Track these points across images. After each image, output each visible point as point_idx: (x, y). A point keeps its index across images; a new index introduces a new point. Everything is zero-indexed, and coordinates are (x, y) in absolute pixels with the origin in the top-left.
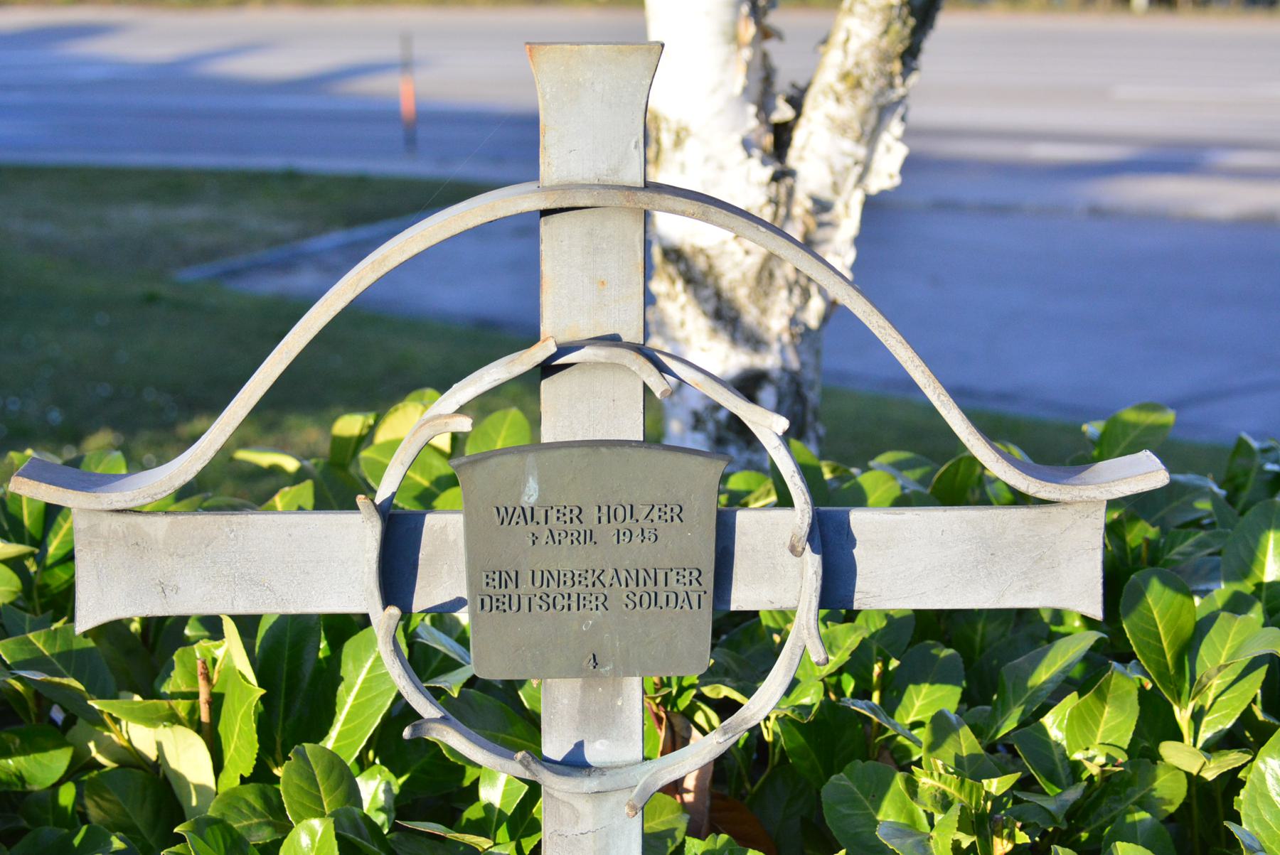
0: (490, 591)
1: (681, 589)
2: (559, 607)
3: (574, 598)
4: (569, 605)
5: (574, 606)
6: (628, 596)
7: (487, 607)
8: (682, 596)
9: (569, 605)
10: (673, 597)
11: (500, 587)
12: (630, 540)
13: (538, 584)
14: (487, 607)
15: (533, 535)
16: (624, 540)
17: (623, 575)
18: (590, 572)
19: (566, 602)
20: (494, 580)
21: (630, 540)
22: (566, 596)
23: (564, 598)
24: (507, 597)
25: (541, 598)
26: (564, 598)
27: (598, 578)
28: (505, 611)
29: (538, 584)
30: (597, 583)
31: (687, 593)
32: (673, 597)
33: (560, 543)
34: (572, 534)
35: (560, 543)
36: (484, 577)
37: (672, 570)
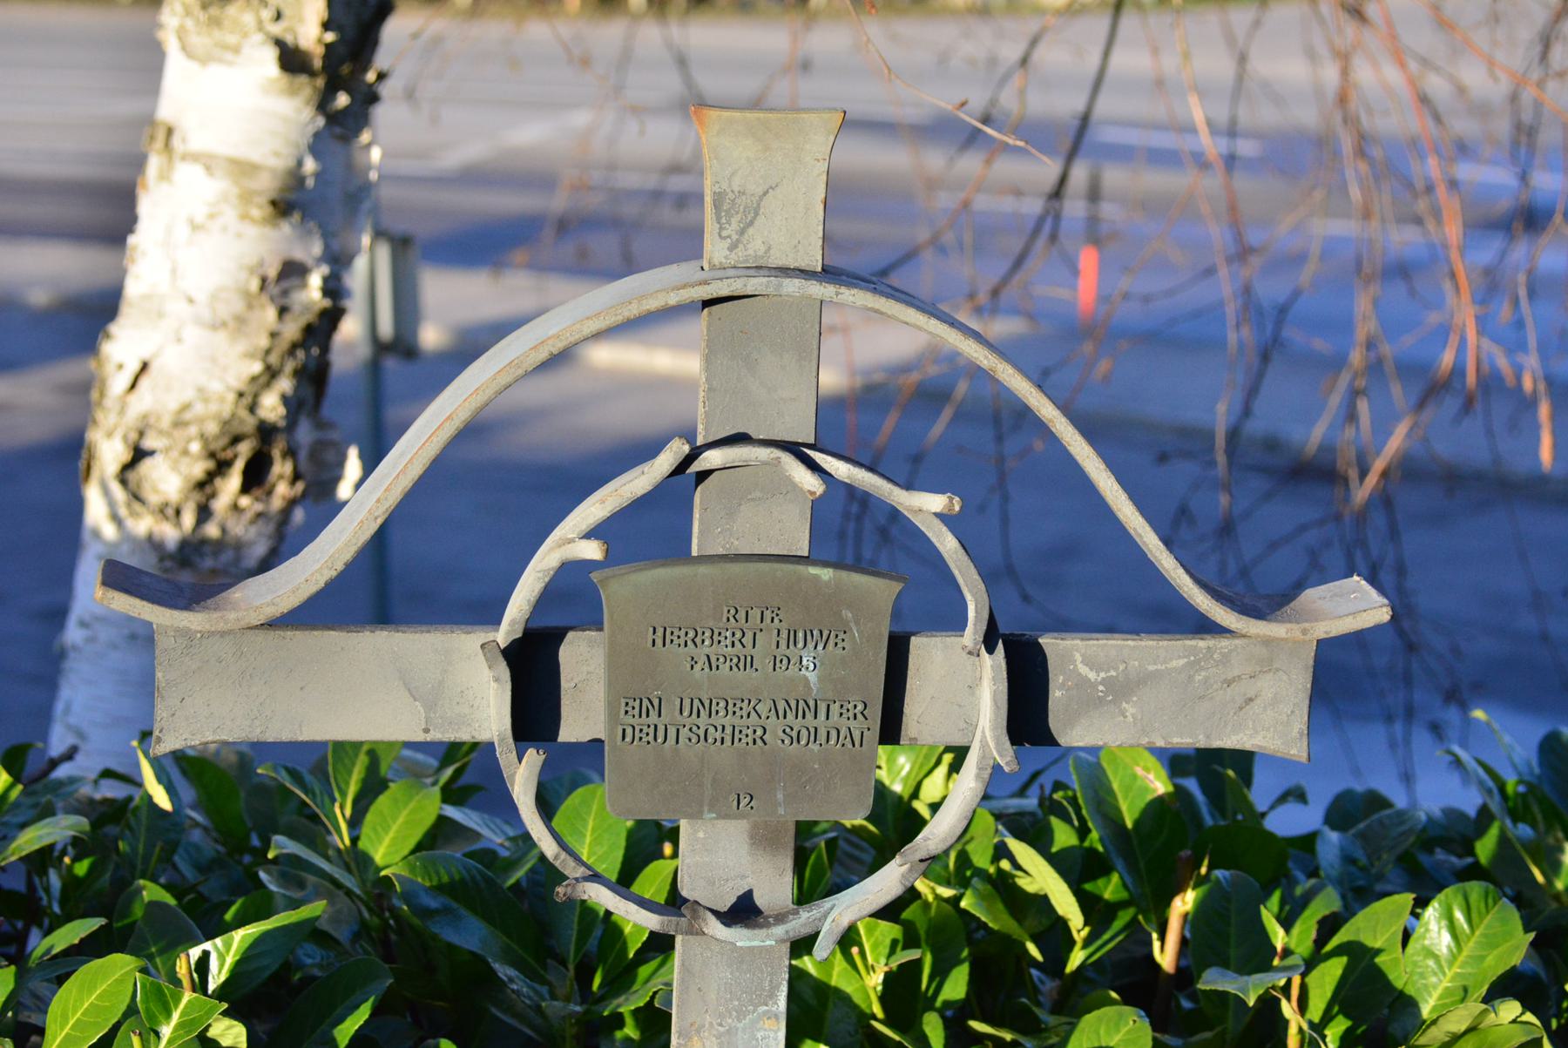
0: (629, 719)
1: (843, 724)
2: (710, 740)
3: (729, 730)
4: (723, 738)
5: (728, 739)
6: (784, 731)
7: (628, 739)
8: (843, 732)
9: (723, 738)
10: (834, 734)
11: (640, 716)
12: (788, 668)
13: (686, 713)
14: (628, 739)
15: (693, 658)
16: (781, 668)
17: (781, 705)
18: (746, 702)
19: (718, 735)
20: (633, 708)
21: (788, 668)
22: (720, 728)
23: (716, 730)
24: (652, 727)
25: (691, 729)
26: (716, 730)
27: (754, 708)
28: (649, 743)
29: (686, 713)
30: (753, 714)
31: (849, 729)
32: (834, 734)
33: (718, 669)
34: (731, 660)
35: (718, 669)
36: (624, 704)
37: (835, 702)
